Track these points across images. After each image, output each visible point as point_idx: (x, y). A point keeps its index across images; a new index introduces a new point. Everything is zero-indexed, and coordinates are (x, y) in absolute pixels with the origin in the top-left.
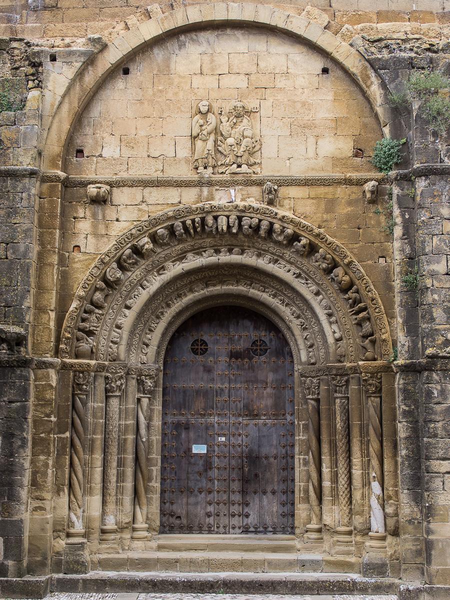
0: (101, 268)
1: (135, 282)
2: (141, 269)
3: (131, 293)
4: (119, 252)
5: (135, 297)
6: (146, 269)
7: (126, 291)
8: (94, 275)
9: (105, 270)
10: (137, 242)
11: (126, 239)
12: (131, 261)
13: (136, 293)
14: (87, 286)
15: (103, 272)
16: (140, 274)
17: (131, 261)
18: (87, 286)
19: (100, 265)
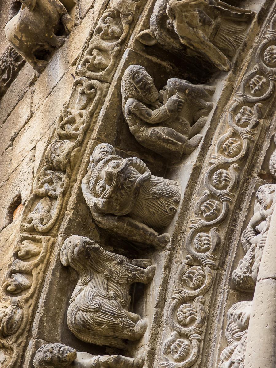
0: (59, 190)
1: (231, 173)
2: (227, 115)
3: (238, 230)
4: (101, 102)
5: (257, 232)
6: (251, 103)
7: (205, 229)
8: (40, 227)
9: (74, 191)
10: (146, 26)
11: (105, 44)
12: (164, 107)
13: (256, 216)
14: (21, 279)
15: (72, 199)
16: (235, 134)
17: (164, 107)
18: (21, 279)
19: (51, 182)
